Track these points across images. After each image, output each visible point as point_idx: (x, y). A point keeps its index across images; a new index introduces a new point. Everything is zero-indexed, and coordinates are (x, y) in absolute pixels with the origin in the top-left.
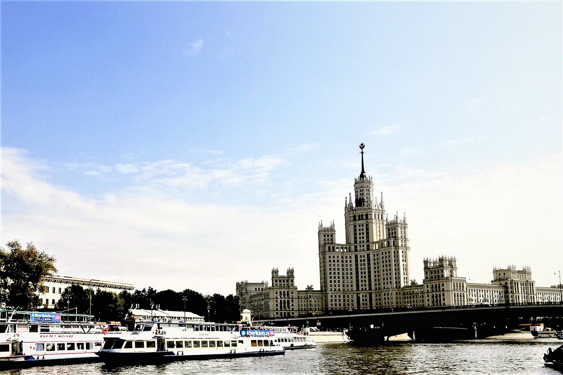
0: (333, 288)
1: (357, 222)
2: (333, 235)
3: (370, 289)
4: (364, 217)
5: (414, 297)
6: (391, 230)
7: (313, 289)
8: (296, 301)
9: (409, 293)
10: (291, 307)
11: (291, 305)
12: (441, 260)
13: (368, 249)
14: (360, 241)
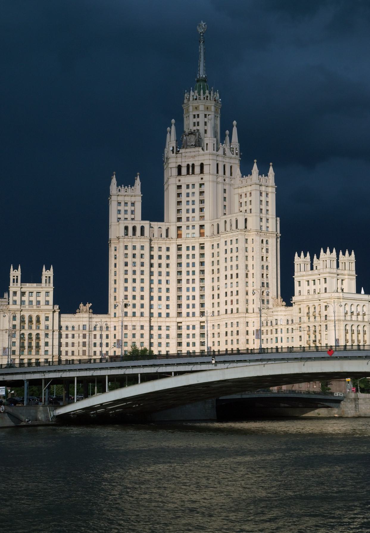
1: (185, 180)
3: (202, 314)
4: (197, 170)
5: (276, 330)
6: (243, 195)
9: (269, 324)
10: (42, 349)
11: (42, 343)
13: (202, 235)
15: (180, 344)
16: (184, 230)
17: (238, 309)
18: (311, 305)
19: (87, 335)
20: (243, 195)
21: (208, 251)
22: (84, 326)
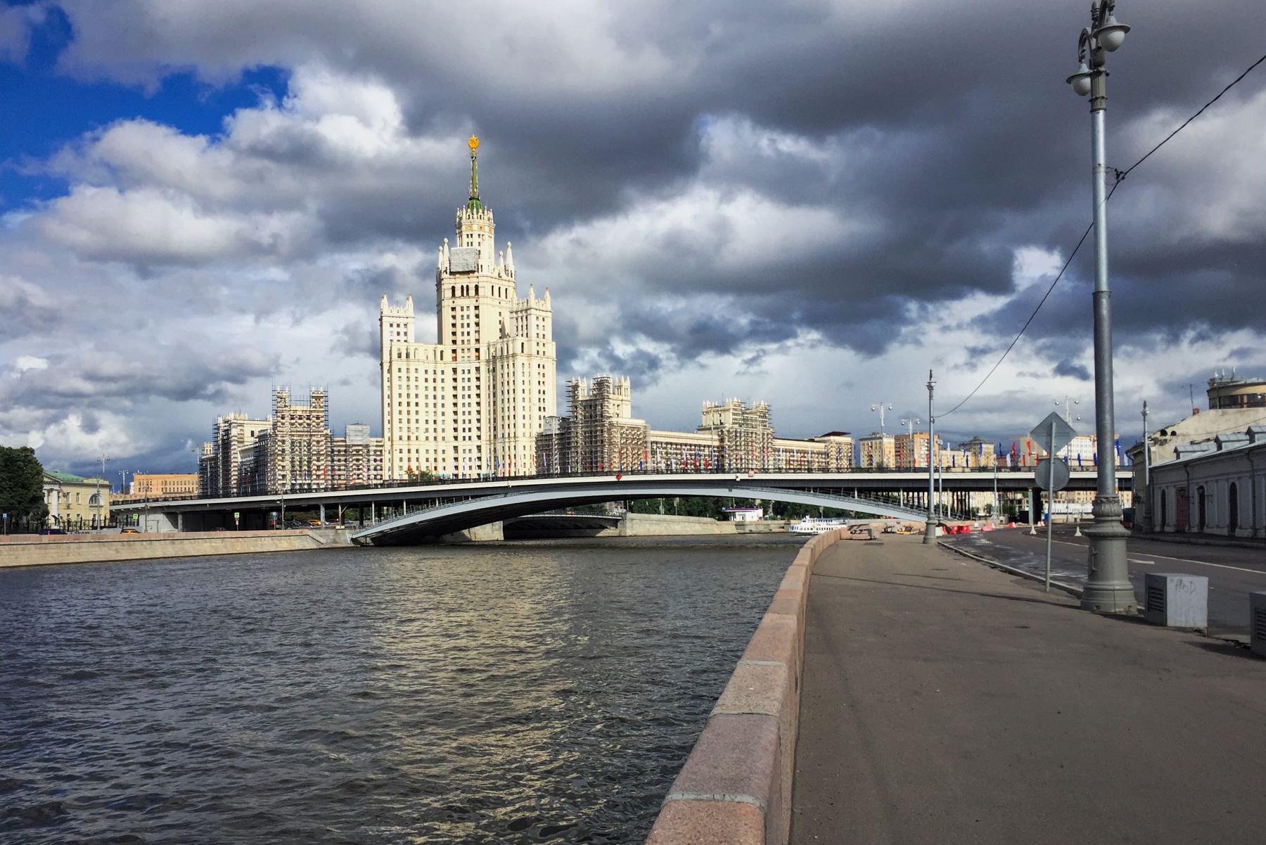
1: (461, 302)
4: (472, 292)
6: (520, 319)
20: (520, 319)
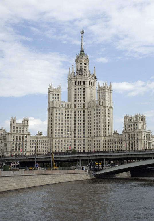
0: (58, 135)
1: (77, 87)
2: (60, 95)
4: (82, 83)
5: (115, 143)
6: (101, 93)
7: (42, 135)
8: (28, 144)
10: (24, 149)
12: (136, 117)
13: (84, 107)
14: (79, 101)
15: (75, 148)
16: (77, 105)
17: (99, 135)
18: (130, 134)
19: (41, 144)
20: (101, 93)
21: (86, 113)
22: (40, 140)
